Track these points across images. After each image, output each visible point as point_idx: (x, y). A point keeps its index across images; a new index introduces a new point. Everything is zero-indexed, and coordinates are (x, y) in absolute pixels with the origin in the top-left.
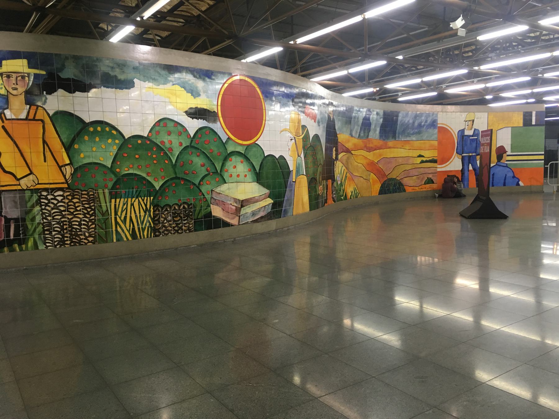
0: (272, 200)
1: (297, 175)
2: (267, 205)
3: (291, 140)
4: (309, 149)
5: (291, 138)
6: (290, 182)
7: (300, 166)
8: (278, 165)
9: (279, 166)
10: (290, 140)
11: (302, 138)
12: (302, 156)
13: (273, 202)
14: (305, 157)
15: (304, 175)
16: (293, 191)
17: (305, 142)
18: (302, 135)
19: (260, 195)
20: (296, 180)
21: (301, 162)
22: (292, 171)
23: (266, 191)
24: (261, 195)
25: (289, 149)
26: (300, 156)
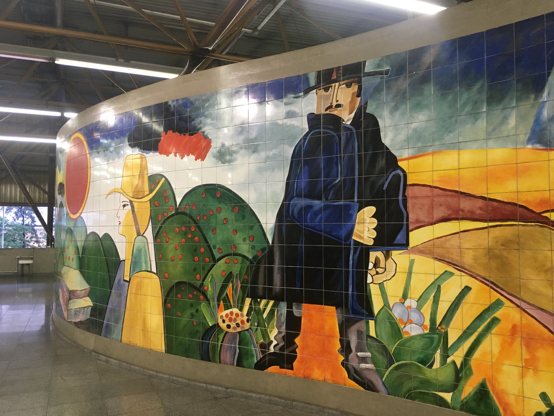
0: (92, 301)
1: (133, 271)
2: (86, 307)
3: (124, 206)
4: (170, 220)
5: (125, 203)
6: (119, 280)
7: (143, 253)
8: (102, 248)
9: (102, 251)
10: (122, 208)
11: (150, 200)
12: (149, 234)
13: (92, 305)
14: (155, 237)
15: (151, 272)
16: (123, 298)
17: (156, 207)
18: (148, 195)
19: (81, 289)
20: (130, 279)
21: (144, 246)
22: (124, 261)
23: (87, 286)
24: (81, 290)
25: (119, 222)
26: (142, 235)
